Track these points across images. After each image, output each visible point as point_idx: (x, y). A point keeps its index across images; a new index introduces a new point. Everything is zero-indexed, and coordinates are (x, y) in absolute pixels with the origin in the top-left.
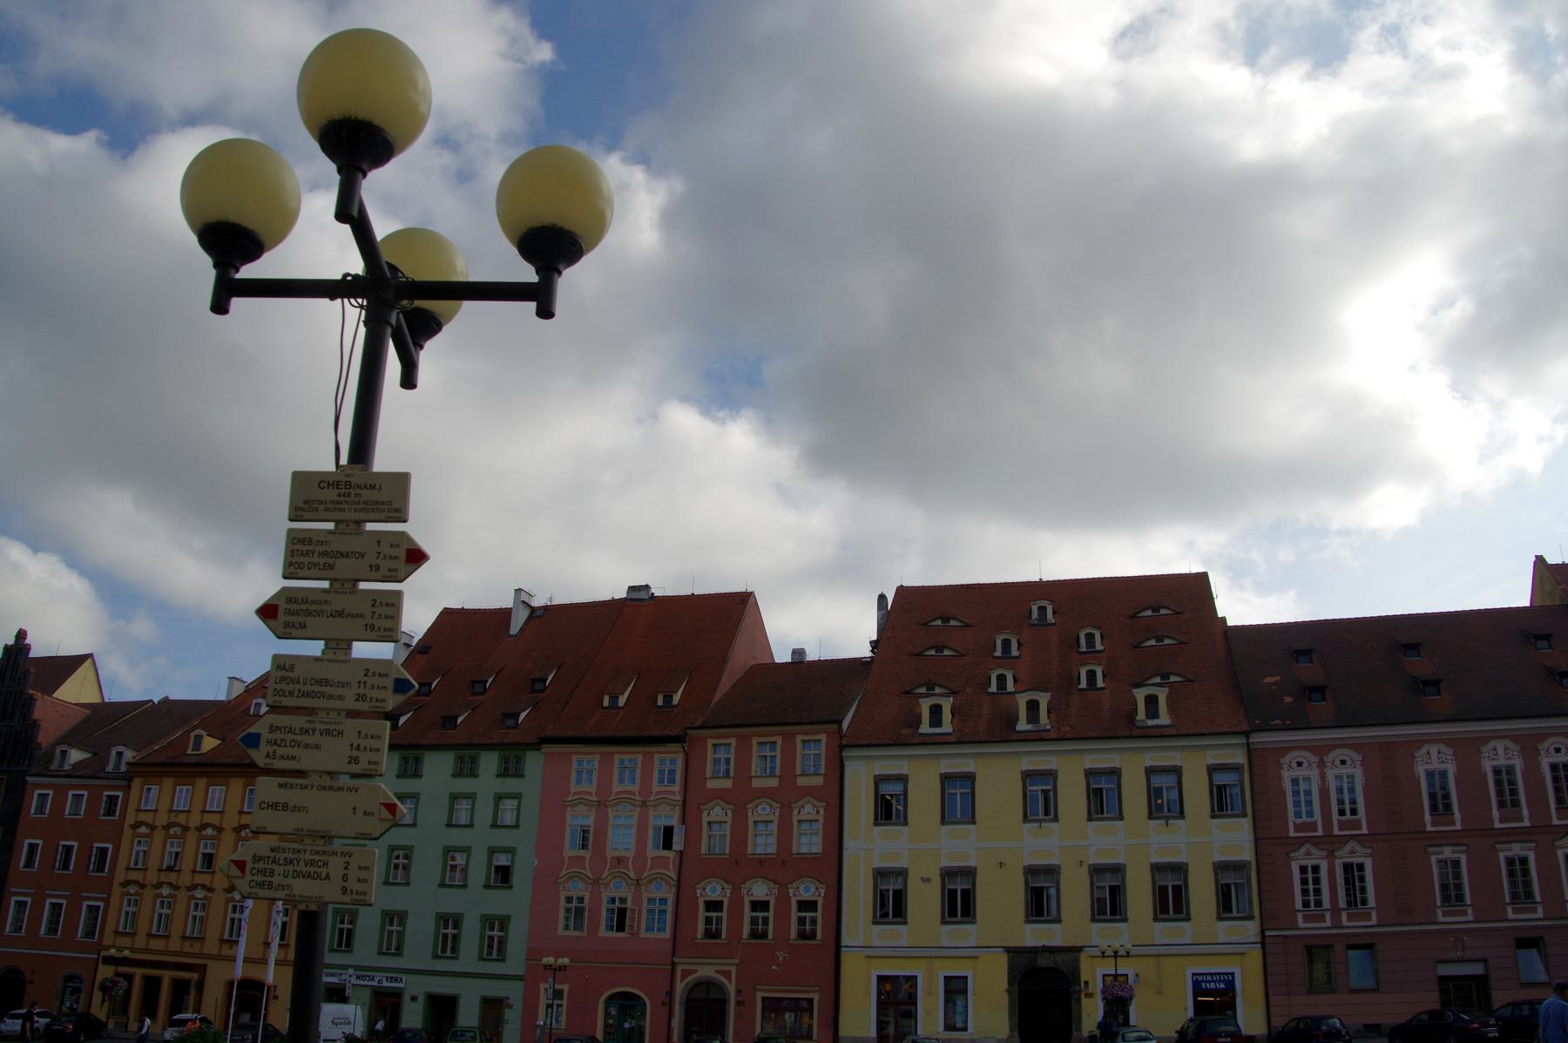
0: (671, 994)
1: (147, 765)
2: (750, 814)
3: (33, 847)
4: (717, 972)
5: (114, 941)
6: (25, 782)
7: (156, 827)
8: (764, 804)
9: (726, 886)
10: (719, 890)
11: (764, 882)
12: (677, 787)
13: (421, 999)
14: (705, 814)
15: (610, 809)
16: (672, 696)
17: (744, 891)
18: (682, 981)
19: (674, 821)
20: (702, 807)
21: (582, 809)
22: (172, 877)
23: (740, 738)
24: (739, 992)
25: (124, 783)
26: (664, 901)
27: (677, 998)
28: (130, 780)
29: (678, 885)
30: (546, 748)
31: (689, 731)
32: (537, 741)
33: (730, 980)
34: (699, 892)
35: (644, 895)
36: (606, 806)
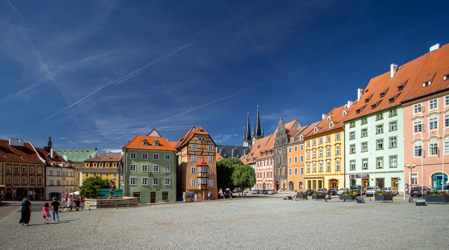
3: (290, 158)
5: (307, 174)
7: (310, 150)
22: (315, 159)
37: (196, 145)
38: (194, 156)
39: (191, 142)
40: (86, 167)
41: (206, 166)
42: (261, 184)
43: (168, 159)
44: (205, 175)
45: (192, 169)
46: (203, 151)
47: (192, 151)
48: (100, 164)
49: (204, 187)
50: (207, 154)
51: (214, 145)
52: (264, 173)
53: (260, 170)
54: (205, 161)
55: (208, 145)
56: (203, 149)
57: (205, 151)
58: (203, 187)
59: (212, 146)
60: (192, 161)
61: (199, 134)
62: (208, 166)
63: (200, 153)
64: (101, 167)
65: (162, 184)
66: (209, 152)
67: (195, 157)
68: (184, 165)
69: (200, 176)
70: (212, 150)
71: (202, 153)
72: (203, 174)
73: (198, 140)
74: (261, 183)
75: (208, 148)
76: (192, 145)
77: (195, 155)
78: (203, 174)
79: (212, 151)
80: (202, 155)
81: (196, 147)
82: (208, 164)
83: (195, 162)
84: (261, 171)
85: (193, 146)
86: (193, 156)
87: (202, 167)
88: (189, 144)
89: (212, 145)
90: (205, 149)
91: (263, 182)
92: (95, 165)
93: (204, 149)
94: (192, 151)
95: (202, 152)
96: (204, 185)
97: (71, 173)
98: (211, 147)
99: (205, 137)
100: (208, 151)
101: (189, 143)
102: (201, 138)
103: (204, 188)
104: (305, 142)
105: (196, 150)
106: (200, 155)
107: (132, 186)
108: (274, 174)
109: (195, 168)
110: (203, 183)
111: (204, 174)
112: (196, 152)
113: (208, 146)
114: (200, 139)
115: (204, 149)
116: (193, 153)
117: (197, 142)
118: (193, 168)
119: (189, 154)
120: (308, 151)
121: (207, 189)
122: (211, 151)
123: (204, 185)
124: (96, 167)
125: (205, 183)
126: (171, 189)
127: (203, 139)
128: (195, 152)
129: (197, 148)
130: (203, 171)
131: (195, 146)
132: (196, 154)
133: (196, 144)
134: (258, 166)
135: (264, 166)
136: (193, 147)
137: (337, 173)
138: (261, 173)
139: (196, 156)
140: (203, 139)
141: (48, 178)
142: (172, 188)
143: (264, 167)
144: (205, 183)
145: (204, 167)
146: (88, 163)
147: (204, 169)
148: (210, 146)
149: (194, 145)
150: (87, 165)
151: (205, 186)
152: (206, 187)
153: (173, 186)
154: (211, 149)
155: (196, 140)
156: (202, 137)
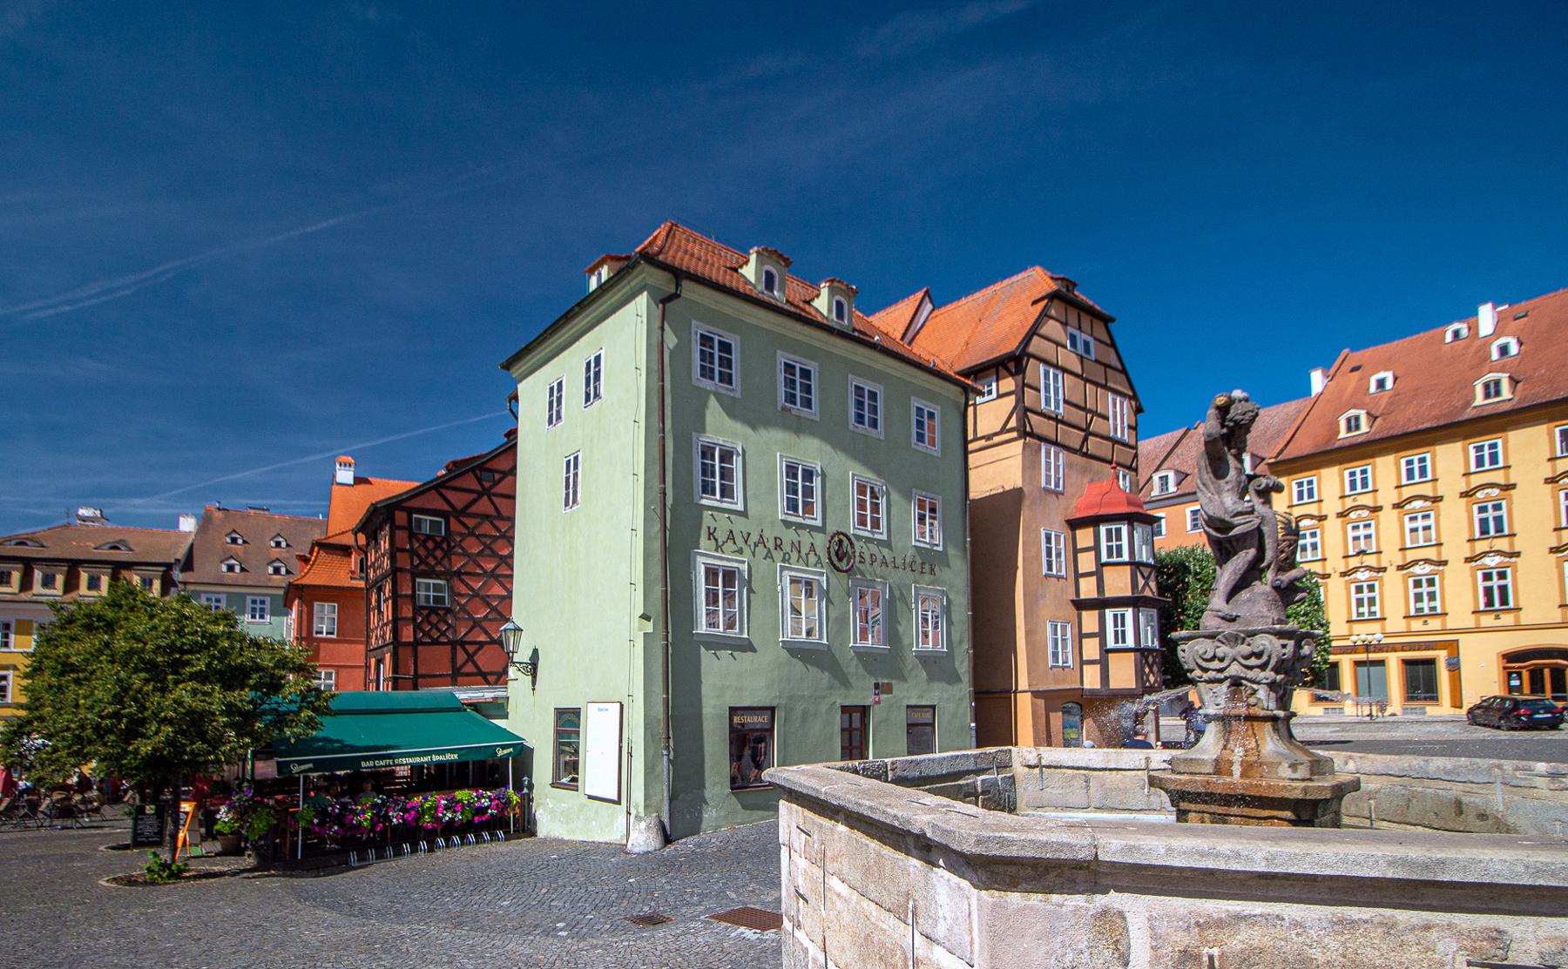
55: (1105, 387)
56: (1090, 411)
58: (1147, 670)
60: (1043, 484)
65: (906, 642)
68: (1008, 504)
71: (1085, 439)
72: (1141, 582)
73: (1064, 342)
77: (1055, 443)
80: (1084, 450)
83: (1057, 494)
99: (1092, 335)
100: (1112, 434)
105: (1061, 411)
107: (715, 644)
112: (1062, 422)
114: (1073, 338)
119: (1028, 429)
123: (1150, 659)
126: (949, 683)
132: (1063, 442)
133: (1056, 367)
139: (1061, 455)
142: (954, 678)
153: (957, 664)
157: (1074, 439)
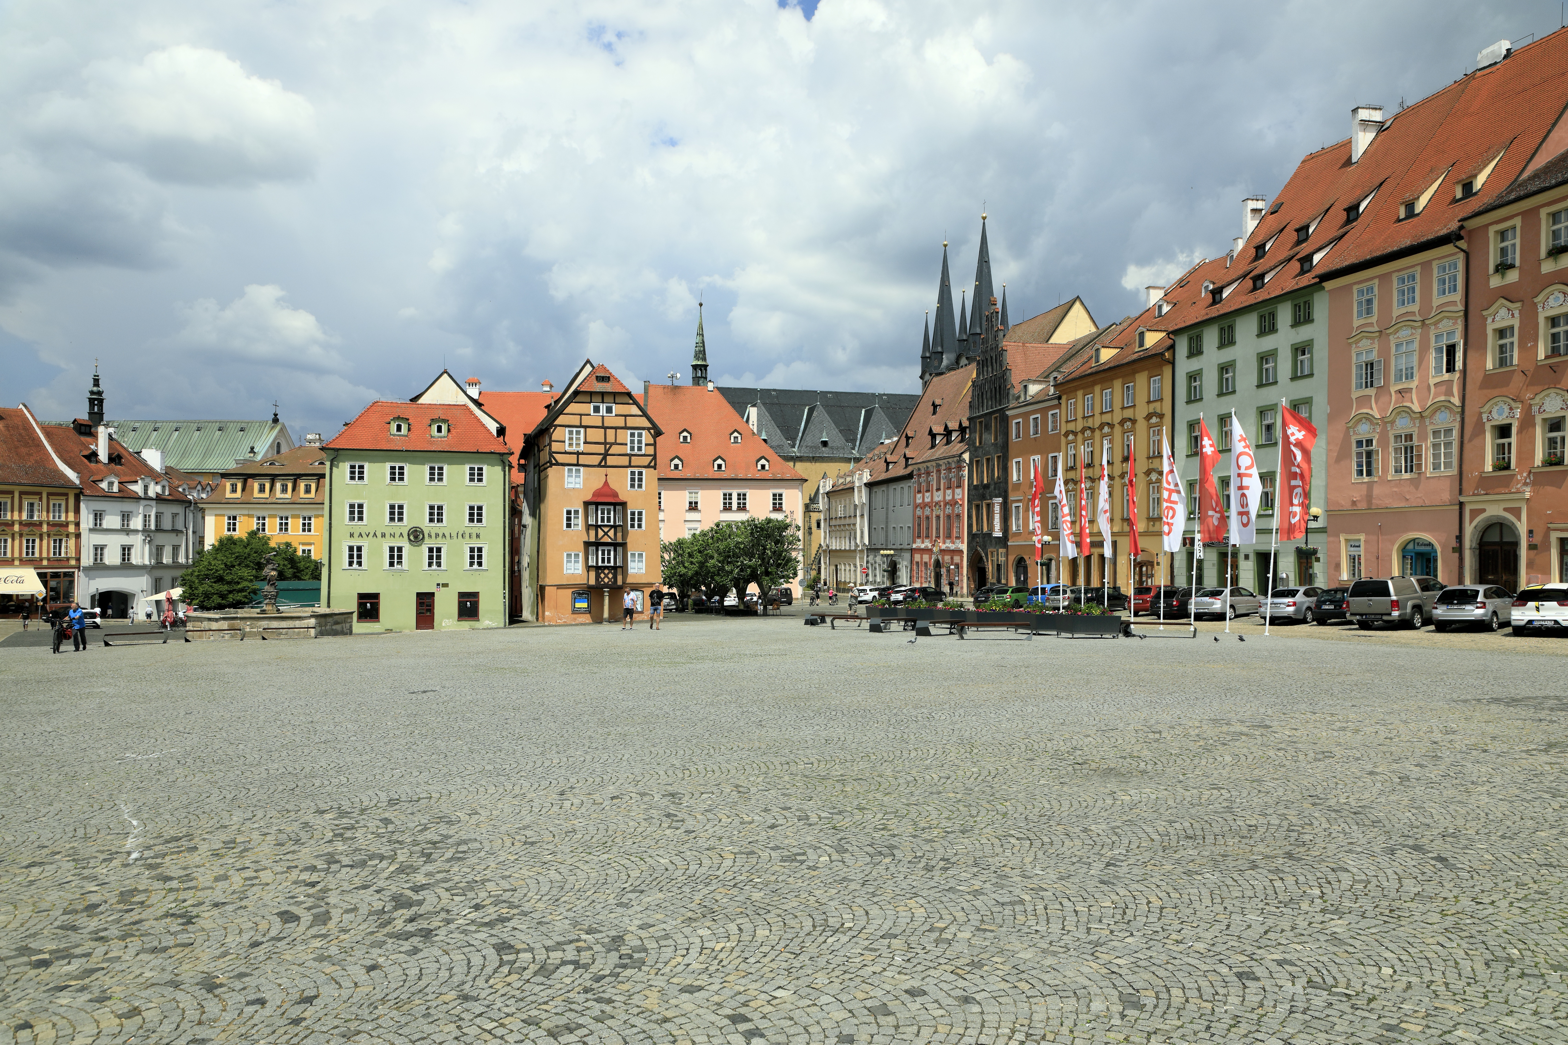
0: (1460, 538)
1: (1068, 381)
2: (1540, 309)
4: (1505, 509)
6: (1007, 416)
8: (1556, 293)
9: (1513, 404)
10: (1506, 409)
11: (1557, 394)
12: (1458, 297)
13: (1252, 556)
14: (1490, 320)
15: (1391, 337)
16: (1471, 183)
17: (1535, 409)
18: (1471, 522)
19: (1458, 339)
20: (1484, 313)
21: (1365, 343)
23: (1524, 214)
24: (1530, 532)
25: (1056, 402)
26: (1448, 432)
27: (1467, 543)
28: (1059, 398)
29: (1463, 412)
30: (1329, 285)
31: (1465, 224)
32: (1317, 280)
33: (1519, 519)
34: (1485, 416)
35: (1429, 428)
36: (1388, 335)
37: (582, 430)
38: (574, 468)
39: (561, 420)
40: (228, 495)
41: (615, 504)
42: (926, 563)
43: (480, 480)
44: (611, 533)
45: (565, 516)
46: (607, 451)
47: (566, 453)
48: (278, 486)
49: (606, 576)
50: (625, 461)
51: (648, 429)
52: (938, 517)
53: (924, 505)
54: (613, 485)
55: (626, 428)
57: (614, 450)
59: (644, 432)
61: (591, 394)
62: (624, 504)
63: (596, 460)
64: (283, 496)
66: (630, 456)
67: (578, 471)
69: (592, 539)
70: (643, 445)
71: (604, 459)
74: (926, 558)
75: (629, 438)
76: (567, 429)
77: (577, 465)
78: (601, 533)
79: (643, 452)
81: (582, 436)
82: (622, 497)
84: (927, 511)
85: (571, 433)
86: (570, 471)
87: (600, 507)
88: (556, 426)
89: (643, 429)
90: (616, 443)
91: (934, 557)
92: (262, 489)
93: (612, 444)
94: (566, 453)
95: (606, 455)
96: (606, 571)
97: (175, 515)
98: (640, 435)
100: (629, 452)
101: (556, 423)
102: (601, 405)
103: (606, 580)
104: (1064, 398)
106: (597, 463)
108: (970, 526)
109: (576, 512)
110: (603, 561)
111: (606, 534)
113: (629, 432)
115: (612, 444)
116: (573, 459)
117: (586, 421)
118: (569, 512)
120: (1071, 437)
121: (620, 582)
122: (640, 449)
124: (267, 494)
125: (612, 564)
127: (609, 410)
128: (578, 454)
129: (586, 442)
130: (603, 520)
131: (578, 433)
133: (581, 426)
134: (919, 492)
135: (938, 489)
136: (571, 439)
137: (1151, 529)
138: (928, 518)
140: (609, 410)
141: (89, 540)
143: (938, 497)
144: (612, 564)
145: (606, 507)
146: (233, 481)
147: (609, 513)
148: (636, 432)
149: (574, 430)
150: (234, 490)
151: (610, 576)
152: (615, 577)
154: (640, 442)
155: (581, 415)
156: (603, 402)
157: (596, 460)
